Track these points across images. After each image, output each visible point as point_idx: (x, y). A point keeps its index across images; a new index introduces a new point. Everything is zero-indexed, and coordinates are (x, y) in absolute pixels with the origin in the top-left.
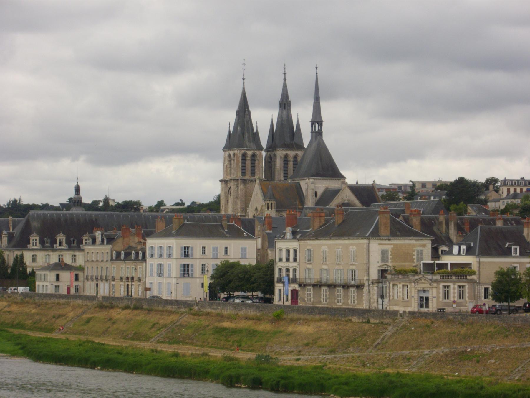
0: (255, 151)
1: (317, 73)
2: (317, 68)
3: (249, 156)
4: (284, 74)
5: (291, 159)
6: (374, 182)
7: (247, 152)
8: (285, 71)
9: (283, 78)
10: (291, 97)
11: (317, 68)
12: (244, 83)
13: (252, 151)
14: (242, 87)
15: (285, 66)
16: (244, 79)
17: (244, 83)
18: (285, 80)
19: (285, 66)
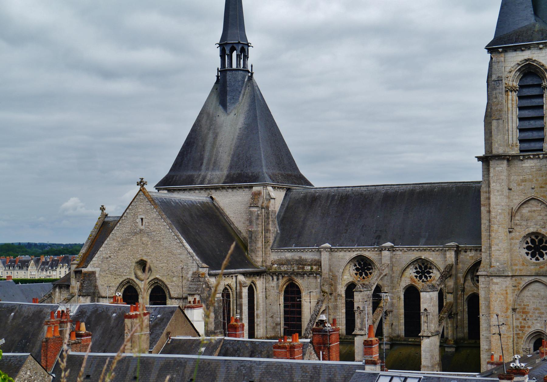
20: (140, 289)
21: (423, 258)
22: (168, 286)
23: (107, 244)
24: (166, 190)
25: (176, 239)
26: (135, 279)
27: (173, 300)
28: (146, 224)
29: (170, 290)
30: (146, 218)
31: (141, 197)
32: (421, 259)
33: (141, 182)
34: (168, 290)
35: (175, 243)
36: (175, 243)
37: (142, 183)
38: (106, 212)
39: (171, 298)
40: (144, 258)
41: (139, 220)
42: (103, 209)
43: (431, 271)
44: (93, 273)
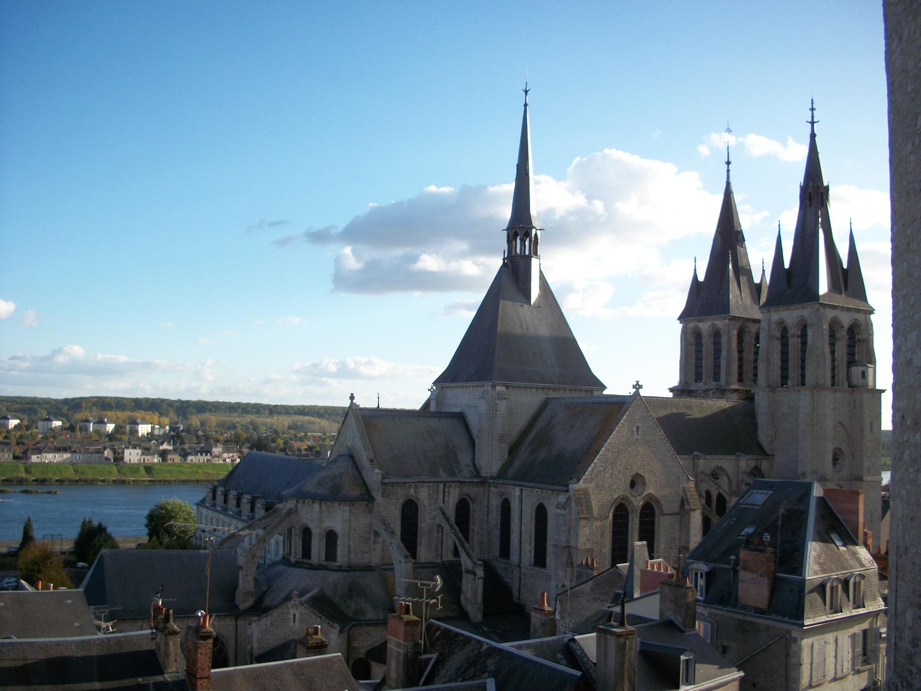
0: (716, 322)
1: (526, 105)
2: (526, 92)
3: (705, 334)
4: (810, 125)
5: (794, 331)
6: (638, 386)
7: (701, 325)
8: (813, 117)
9: (810, 132)
10: (827, 178)
11: (526, 92)
12: (728, 171)
13: (709, 323)
14: (725, 180)
15: (812, 104)
16: (728, 163)
17: (728, 171)
18: (813, 136)
19: (812, 104)
20: (635, 507)
21: (719, 466)
22: (661, 502)
23: (601, 455)
24: (504, 386)
25: (670, 451)
26: (630, 496)
27: (665, 517)
28: (643, 433)
29: (662, 505)
30: (642, 426)
31: (638, 403)
32: (718, 467)
33: (639, 385)
34: (661, 505)
35: (669, 455)
36: (669, 455)
37: (637, 387)
38: (354, 401)
39: (663, 514)
40: (641, 472)
41: (635, 429)
42: (352, 397)
43: (719, 477)
44: (587, 489)
